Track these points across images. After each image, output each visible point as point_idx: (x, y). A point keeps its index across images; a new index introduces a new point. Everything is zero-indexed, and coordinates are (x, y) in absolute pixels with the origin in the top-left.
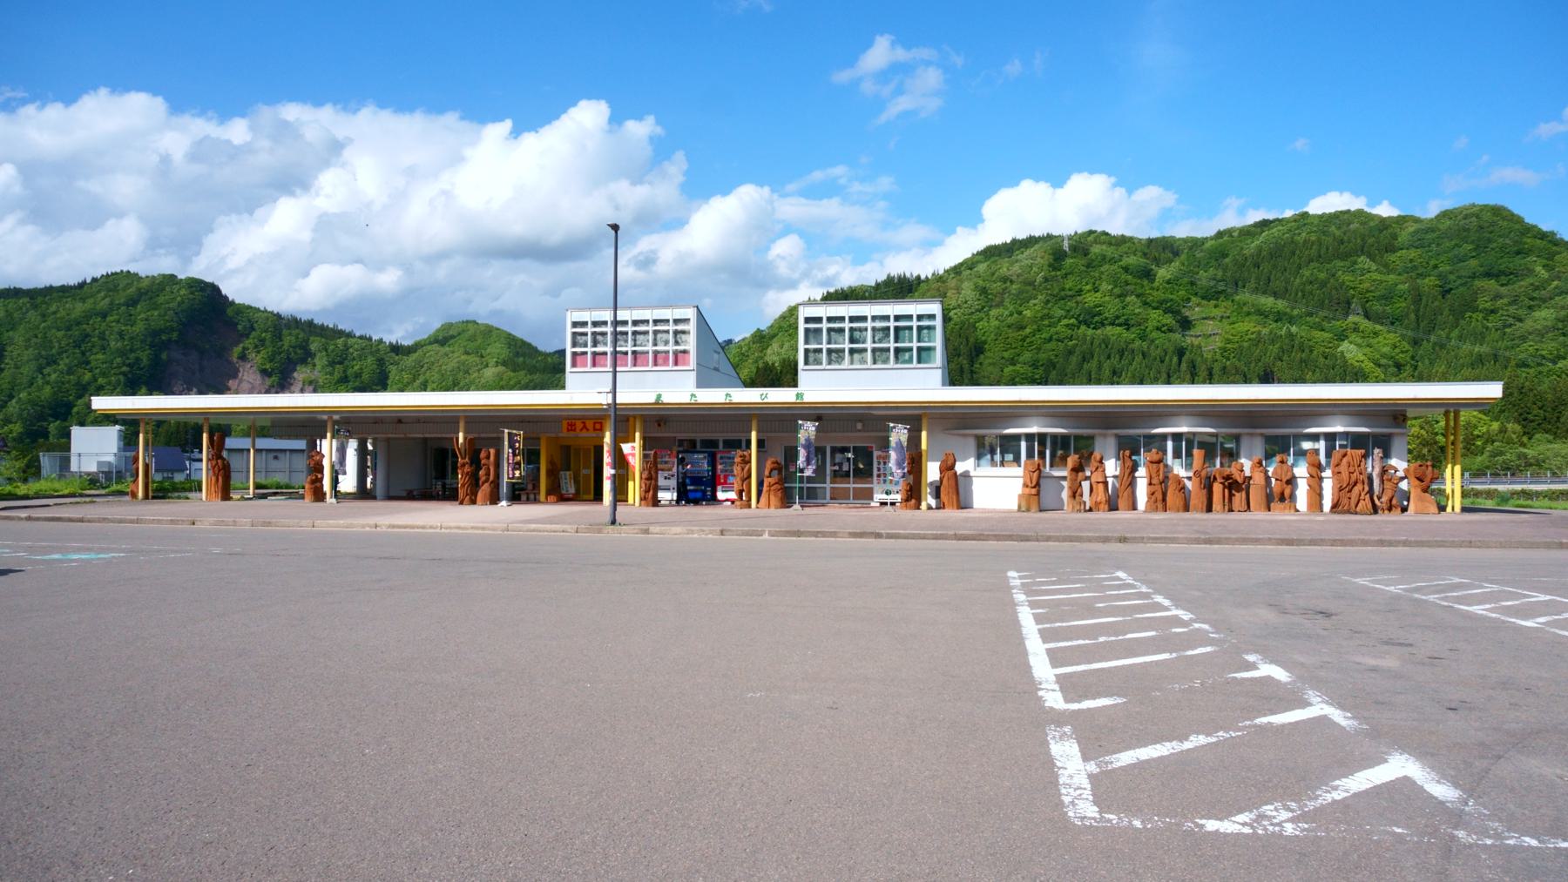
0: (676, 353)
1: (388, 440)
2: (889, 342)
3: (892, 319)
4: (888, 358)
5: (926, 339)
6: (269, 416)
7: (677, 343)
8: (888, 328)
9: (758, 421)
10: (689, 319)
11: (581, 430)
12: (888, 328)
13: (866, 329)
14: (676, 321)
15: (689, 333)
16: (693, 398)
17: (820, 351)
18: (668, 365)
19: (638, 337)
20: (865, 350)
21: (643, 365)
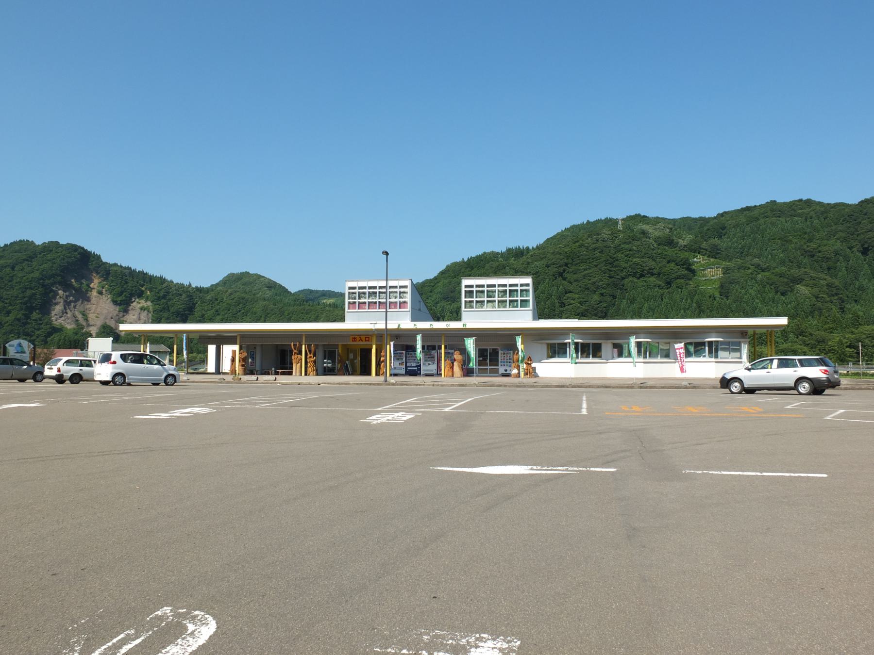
0: (400, 303)
1: (262, 345)
2: (506, 297)
3: (508, 286)
4: (506, 305)
5: (525, 296)
6: (199, 334)
7: (400, 297)
8: (506, 291)
9: (445, 337)
10: (407, 286)
11: (359, 341)
12: (506, 291)
13: (495, 291)
14: (401, 287)
15: (407, 293)
16: (431, 326)
17: (472, 301)
18: (397, 308)
19: (381, 295)
20: (494, 301)
21: (373, 309)
